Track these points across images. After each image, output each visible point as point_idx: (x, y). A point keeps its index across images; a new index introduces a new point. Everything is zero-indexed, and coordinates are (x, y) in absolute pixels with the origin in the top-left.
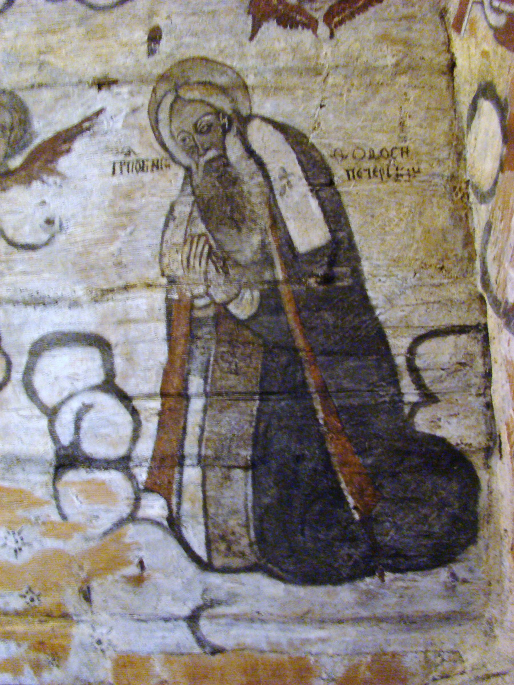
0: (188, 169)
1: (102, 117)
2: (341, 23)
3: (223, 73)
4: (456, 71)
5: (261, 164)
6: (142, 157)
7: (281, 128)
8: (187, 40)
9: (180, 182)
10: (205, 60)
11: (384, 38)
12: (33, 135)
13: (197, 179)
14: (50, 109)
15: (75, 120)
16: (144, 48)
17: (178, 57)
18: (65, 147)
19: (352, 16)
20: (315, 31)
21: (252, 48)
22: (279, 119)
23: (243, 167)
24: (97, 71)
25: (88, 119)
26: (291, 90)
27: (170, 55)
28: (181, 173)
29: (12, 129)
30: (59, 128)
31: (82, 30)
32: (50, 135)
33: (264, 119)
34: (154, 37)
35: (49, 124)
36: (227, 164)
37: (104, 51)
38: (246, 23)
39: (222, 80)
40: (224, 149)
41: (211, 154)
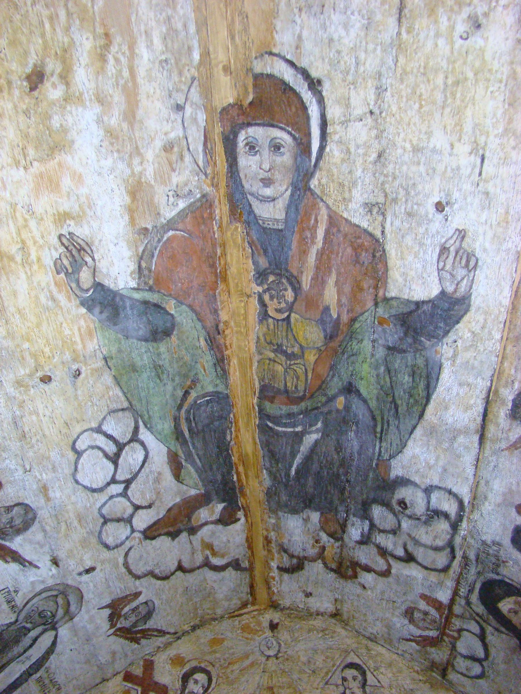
0: (17, 621)
1: (34, 570)
2: (117, 635)
3: (76, 608)
4: (105, 682)
5: (31, 646)
6: (16, 598)
7: (54, 643)
8: (91, 584)
9: (8, 622)
10: (82, 597)
11: (114, 653)
12: (11, 540)
13: (13, 627)
14: (31, 542)
15: (27, 558)
16: (82, 569)
17: (80, 587)
18: (9, 559)
19: (121, 637)
20: (110, 628)
21: (94, 612)
22: (58, 640)
23: (27, 641)
24: (61, 555)
25: (30, 563)
26: (76, 635)
27: (81, 583)
28: (13, 620)
29: (11, 527)
30: (21, 551)
31: (85, 535)
32: (14, 548)
33: (56, 637)
34: (89, 570)
35: (21, 545)
36: (25, 635)
37: (75, 552)
38: (107, 600)
39: (73, 608)
40: (34, 628)
41: (29, 625)
